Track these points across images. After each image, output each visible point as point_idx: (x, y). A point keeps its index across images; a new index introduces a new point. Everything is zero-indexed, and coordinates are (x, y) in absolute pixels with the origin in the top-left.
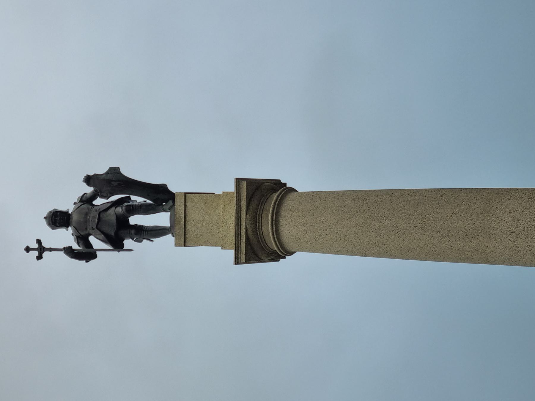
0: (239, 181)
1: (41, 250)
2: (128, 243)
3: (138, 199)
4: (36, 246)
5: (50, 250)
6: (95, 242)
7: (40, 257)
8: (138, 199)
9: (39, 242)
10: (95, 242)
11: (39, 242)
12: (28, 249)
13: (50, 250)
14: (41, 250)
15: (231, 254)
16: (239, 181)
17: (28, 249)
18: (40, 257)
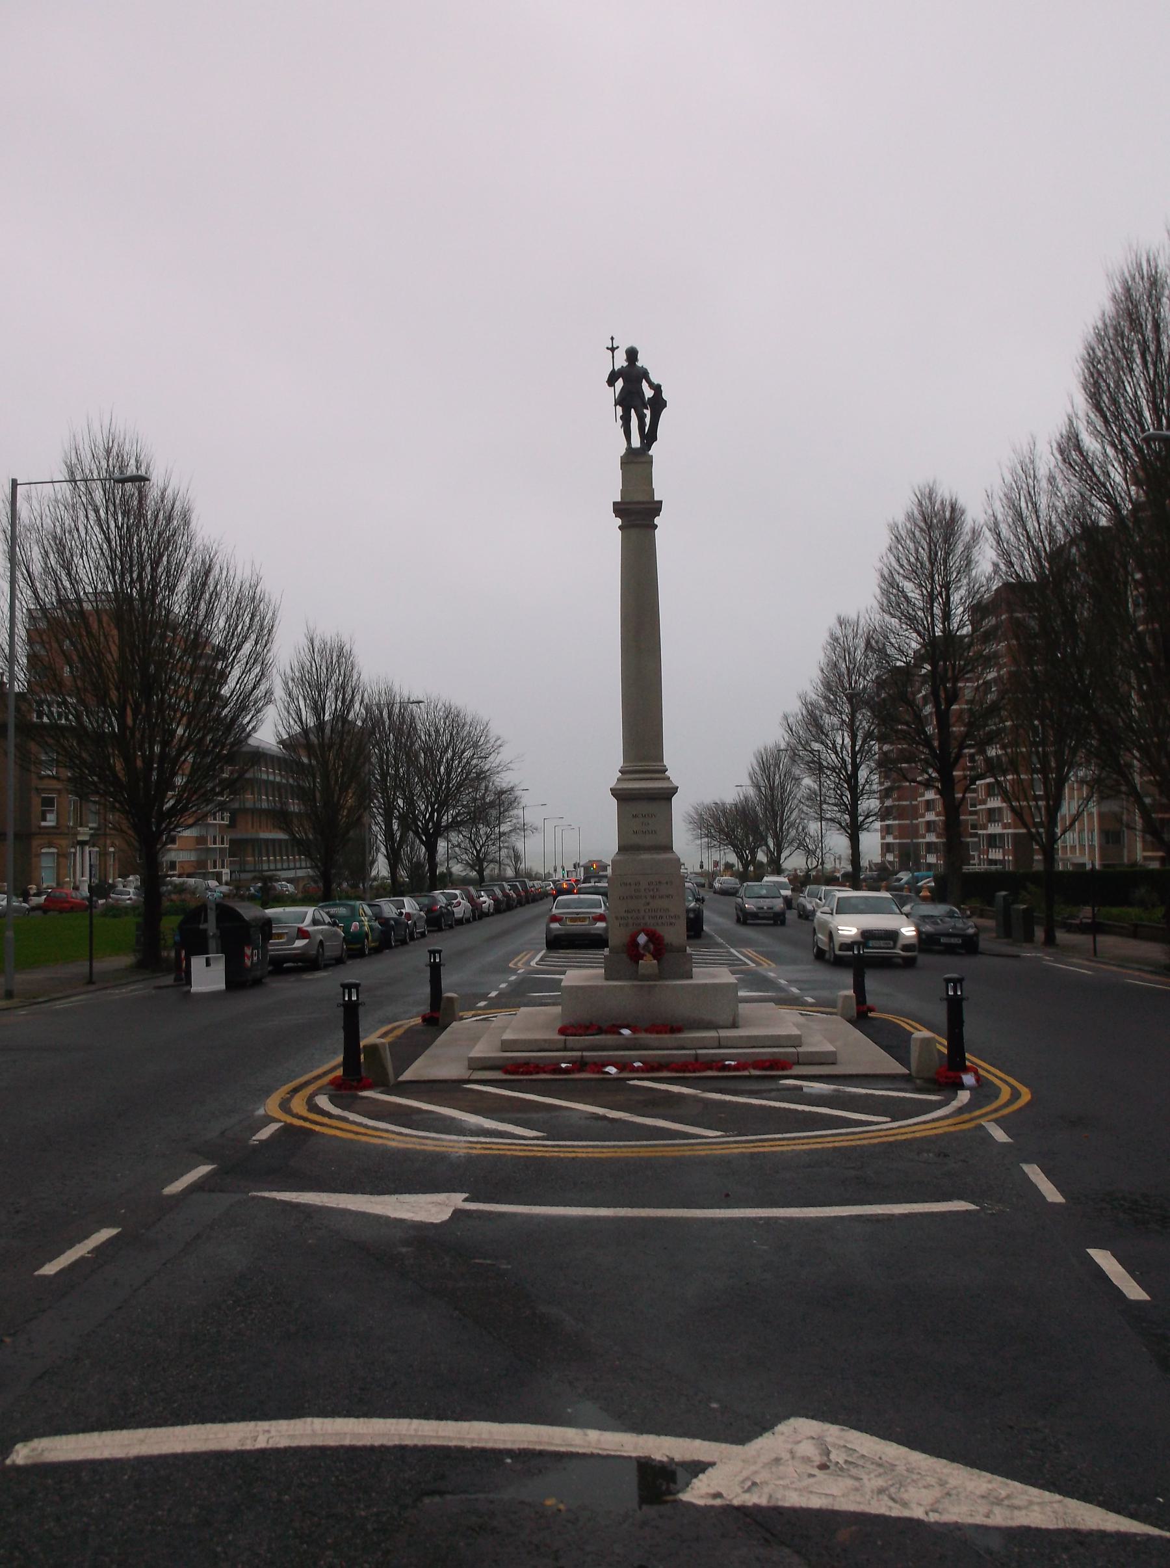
0: (661, 502)
1: (613, 349)
2: (619, 409)
3: (648, 420)
4: (615, 346)
5: (613, 357)
6: (620, 383)
7: (608, 348)
8: (648, 420)
9: (618, 347)
10: (620, 383)
11: (618, 347)
12: (612, 339)
13: (613, 357)
14: (613, 349)
15: (619, 500)
16: (661, 502)
17: (612, 339)
18: (608, 348)
